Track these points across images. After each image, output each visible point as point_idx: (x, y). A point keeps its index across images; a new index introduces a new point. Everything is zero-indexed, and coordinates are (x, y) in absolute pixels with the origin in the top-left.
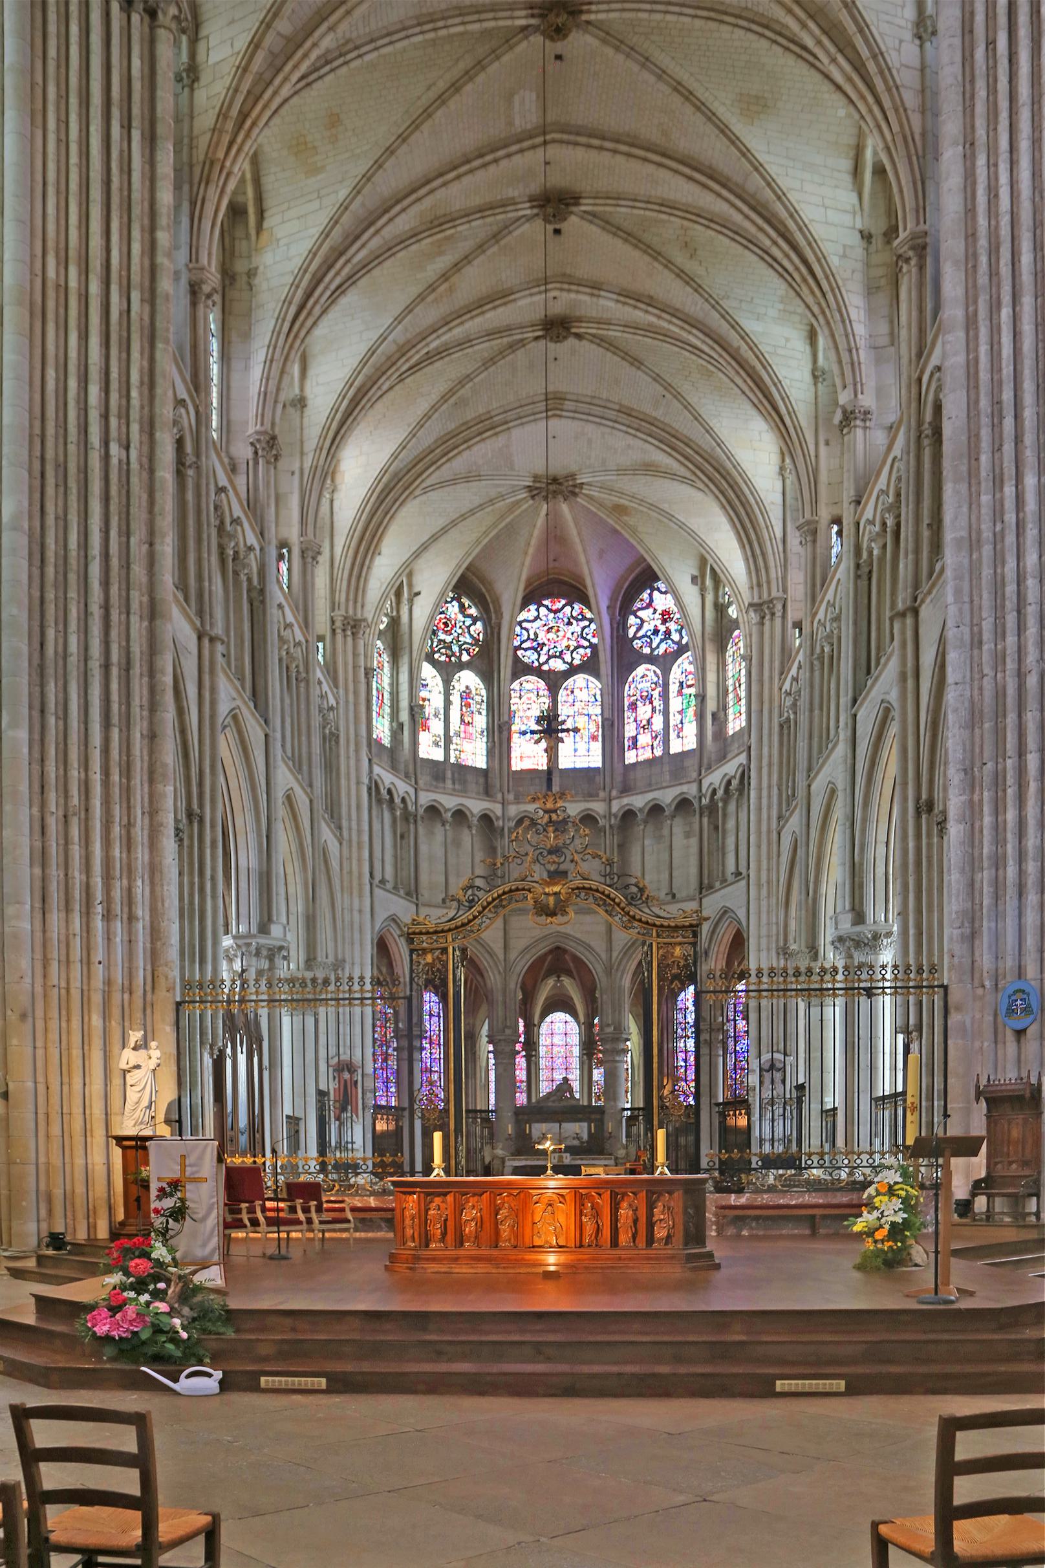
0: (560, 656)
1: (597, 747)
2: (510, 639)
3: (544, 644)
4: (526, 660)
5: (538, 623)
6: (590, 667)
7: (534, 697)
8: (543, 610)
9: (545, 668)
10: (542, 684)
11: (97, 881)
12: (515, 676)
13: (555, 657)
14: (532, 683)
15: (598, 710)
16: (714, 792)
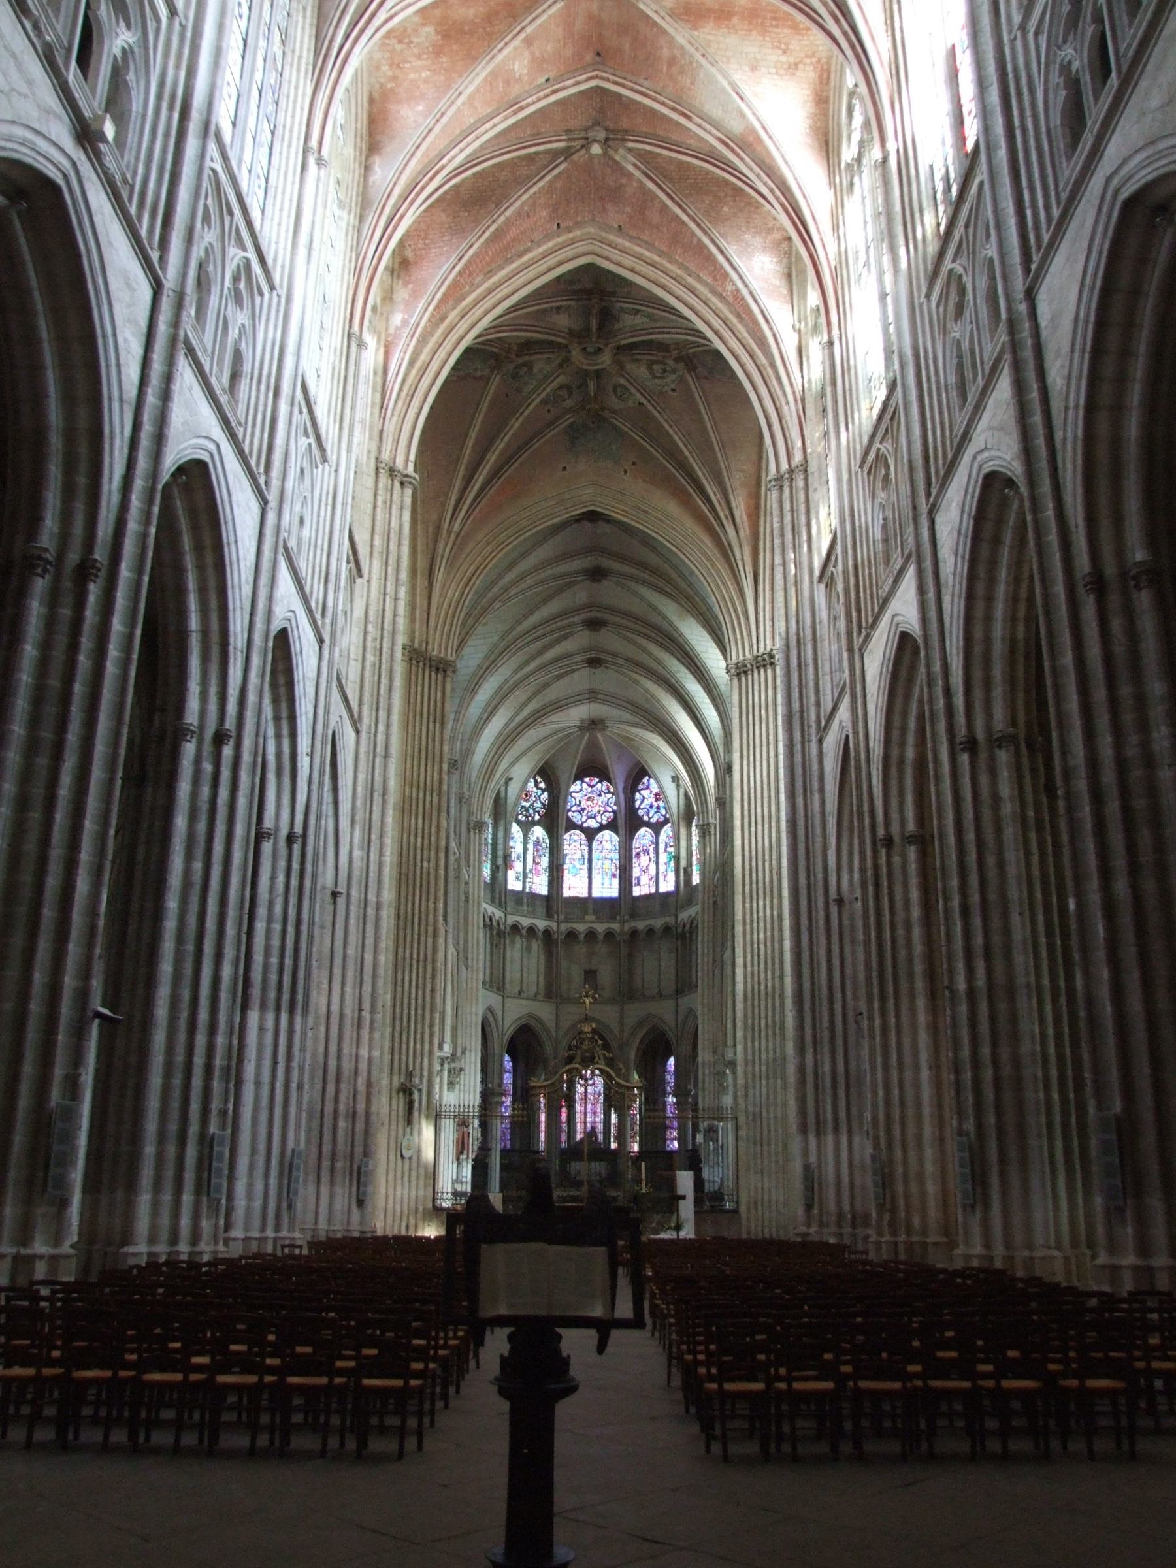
0: (594, 818)
1: (616, 881)
2: (564, 808)
3: (583, 810)
4: (574, 820)
5: (580, 795)
6: (612, 826)
7: (577, 844)
8: (585, 785)
9: (585, 825)
10: (583, 836)
11: (411, 1060)
12: (567, 830)
13: (589, 818)
14: (577, 835)
15: (617, 857)
16: (684, 927)
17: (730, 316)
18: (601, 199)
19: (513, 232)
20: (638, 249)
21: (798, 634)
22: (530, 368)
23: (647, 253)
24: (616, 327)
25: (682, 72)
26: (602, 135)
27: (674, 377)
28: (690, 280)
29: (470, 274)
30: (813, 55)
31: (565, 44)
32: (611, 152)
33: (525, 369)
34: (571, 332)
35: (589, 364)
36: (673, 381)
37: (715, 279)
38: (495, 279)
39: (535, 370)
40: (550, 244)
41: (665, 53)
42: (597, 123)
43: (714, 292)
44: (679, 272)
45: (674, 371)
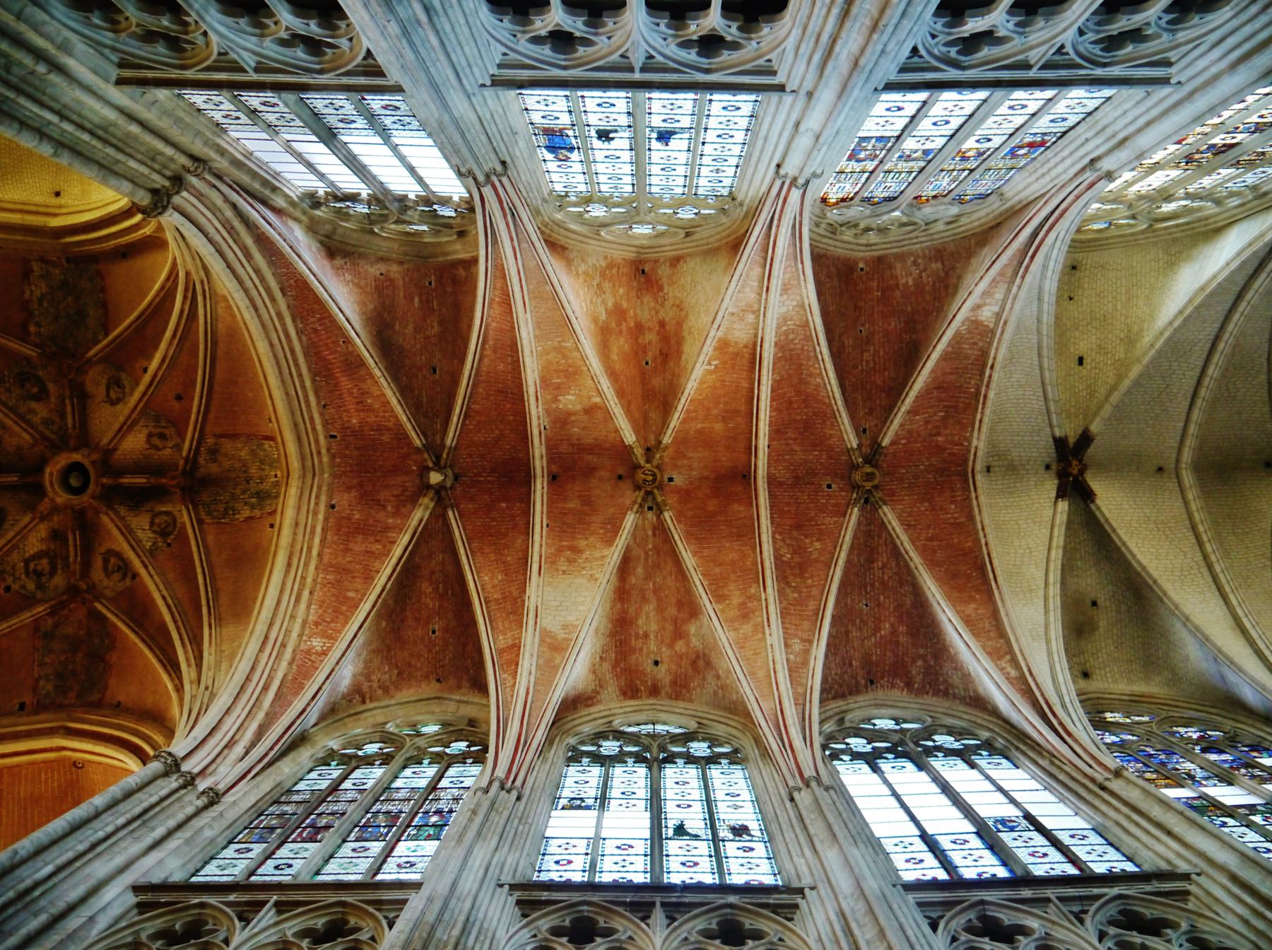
17: (289, 650)
18: (361, 485)
19: (345, 383)
20: (319, 529)
21: (37, 884)
22: (37, 398)
23: (317, 540)
24: (123, 511)
25: (570, 561)
26: (448, 484)
27: (31, 586)
28: (306, 593)
29: (316, 331)
30: (601, 687)
31: (573, 445)
32: (431, 494)
33: (35, 390)
34: (115, 449)
35: (51, 474)
36: (24, 587)
37: (316, 624)
38: (301, 360)
39: (33, 405)
40: (319, 427)
41: (582, 543)
42: (456, 477)
43: (305, 622)
44: (309, 580)
45: (40, 587)
